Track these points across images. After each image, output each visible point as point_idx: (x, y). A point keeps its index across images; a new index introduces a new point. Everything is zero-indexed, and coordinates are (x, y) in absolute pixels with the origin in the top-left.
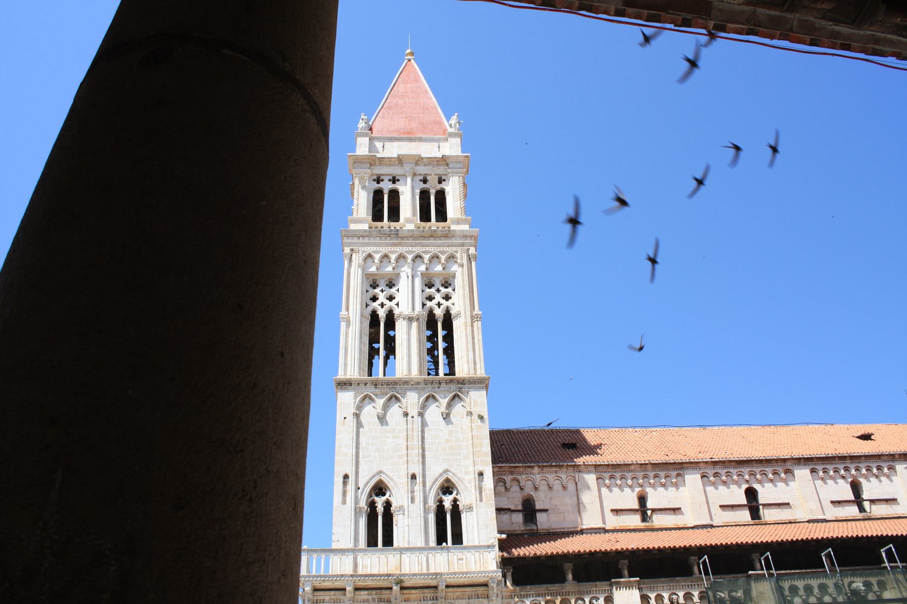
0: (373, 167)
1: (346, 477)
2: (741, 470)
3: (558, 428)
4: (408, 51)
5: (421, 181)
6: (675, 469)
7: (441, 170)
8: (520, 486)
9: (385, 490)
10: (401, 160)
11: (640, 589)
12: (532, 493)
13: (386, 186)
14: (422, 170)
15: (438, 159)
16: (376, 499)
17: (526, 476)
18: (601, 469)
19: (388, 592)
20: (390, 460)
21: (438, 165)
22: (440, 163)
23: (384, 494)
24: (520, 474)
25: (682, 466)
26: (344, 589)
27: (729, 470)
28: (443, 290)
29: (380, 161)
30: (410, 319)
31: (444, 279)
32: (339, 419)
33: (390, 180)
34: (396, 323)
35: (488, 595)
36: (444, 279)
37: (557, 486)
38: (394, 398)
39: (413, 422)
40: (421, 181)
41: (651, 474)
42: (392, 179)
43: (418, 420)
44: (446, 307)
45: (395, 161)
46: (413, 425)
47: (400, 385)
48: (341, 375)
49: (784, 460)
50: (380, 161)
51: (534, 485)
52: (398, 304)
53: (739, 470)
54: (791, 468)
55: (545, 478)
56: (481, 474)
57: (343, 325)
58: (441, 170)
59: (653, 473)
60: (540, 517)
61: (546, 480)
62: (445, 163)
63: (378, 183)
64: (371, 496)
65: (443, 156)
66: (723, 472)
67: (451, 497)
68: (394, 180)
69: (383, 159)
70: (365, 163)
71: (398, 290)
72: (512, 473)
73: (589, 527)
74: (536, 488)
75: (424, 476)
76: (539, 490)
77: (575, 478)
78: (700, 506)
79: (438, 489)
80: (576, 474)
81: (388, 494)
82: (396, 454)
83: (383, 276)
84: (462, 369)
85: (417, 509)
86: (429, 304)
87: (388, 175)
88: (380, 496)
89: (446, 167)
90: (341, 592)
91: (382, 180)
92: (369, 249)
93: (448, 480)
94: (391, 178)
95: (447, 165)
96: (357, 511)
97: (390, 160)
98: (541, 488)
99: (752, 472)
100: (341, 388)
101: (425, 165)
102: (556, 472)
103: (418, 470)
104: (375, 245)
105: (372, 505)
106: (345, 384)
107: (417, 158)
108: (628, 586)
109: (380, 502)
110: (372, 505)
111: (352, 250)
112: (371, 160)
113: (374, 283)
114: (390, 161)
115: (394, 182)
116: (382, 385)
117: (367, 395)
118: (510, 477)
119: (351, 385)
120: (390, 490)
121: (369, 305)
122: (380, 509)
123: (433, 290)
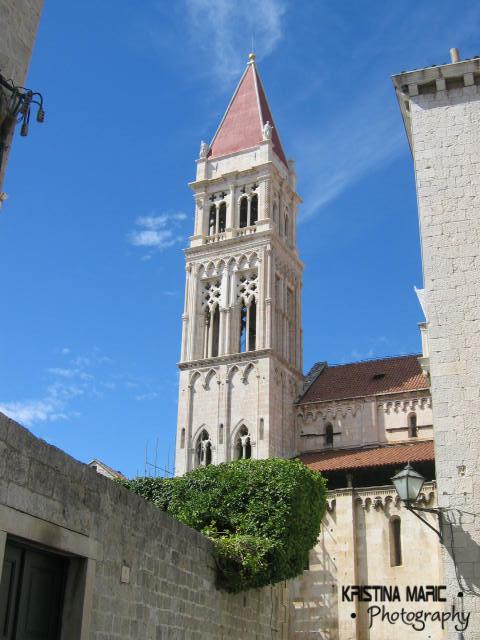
1: (184, 430)
4: (250, 55)
11: (354, 494)
12: (332, 422)
14: (241, 182)
24: (322, 408)
30: (225, 311)
32: (181, 392)
43: (226, 386)
48: (182, 362)
56: (262, 420)
57: (184, 323)
60: (336, 439)
67: (246, 437)
68: (223, 195)
72: (317, 408)
75: (228, 425)
84: (259, 346)
85: (223, 447)
92: (201, 261)
93: (244, 426)
96: (190, 452)
103: (224, 421)
104: (205, 256)
105: (199, 446)
108: (345, 493)
109: (204, 443)
110: (199, 446)
118: (316, 411)
122: (204, 448)
123: (244, 284)
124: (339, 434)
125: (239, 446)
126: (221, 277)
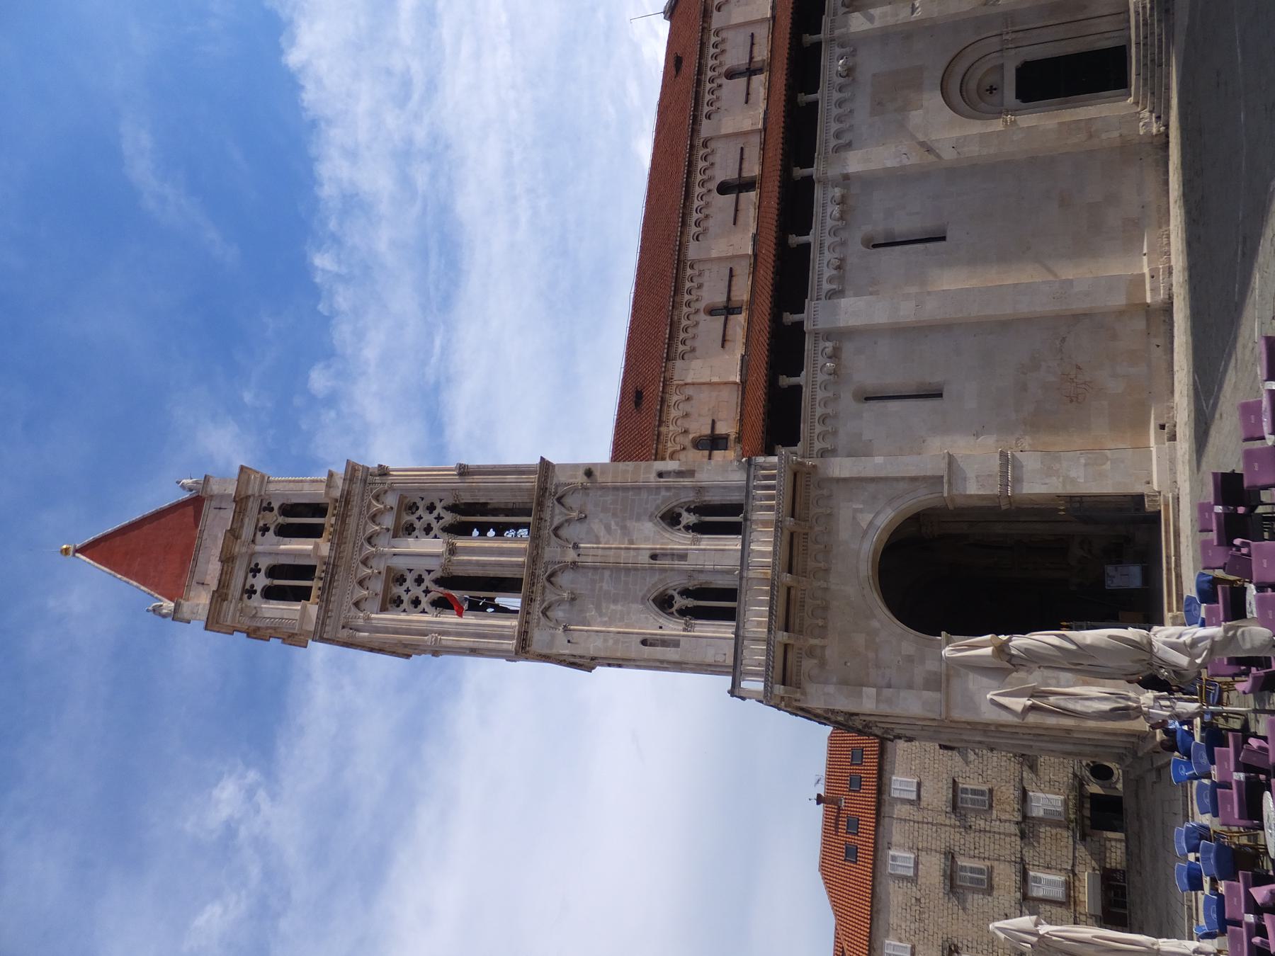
0: (230, 597)
1: (644, 642)
2: (696, 196)
3: (616, 417)
5: (263, 535)
6: (684, 269)
7: (253, 506)
8: (681, 450)
9: (666, 595)
10: (229, 558)
12: (691, 436)
13: (261, 581)
15: (238, 510)
16: (676, 606)
17: (669, 442)
18: (672, 355)
19: (793, 592)
20: (630, 586)
21: (245, 510)
22: (243, 507)
23: (672, 597)
24: (665, 449)
25: (681, 261)
26: (786, 646)
27: (695, 209)
28: (420, 512)
29: (224, 586)
31: (405, 510)
33: (254, 576)
34: (455, 574)
35: (807, 474)
36: (405, 510)
37: (684, 407)
38: (552, 579)
39: (585, 555)
40: (263, 535)
41: (687, 297)
42: (252, 574)
44: (444, 510)
45: (228, 566)
46: (589, 555)
47: (535, 569)
49: (692, 146)
50: (224, 586)
51: (682, 433)
52: (429, 572)
53: (696, 198)
54: (702, 140)
55: (674, 421)
58: (253, 506)
59: (686, 295)
60: (722, 429)
61: (677, 420)
62: (245, 500)
63: (255, 592)
64: (672, 613)
65: (234, 501)
66: (695, 216)
67: (685, 514)
69: (222, 583)
70: (221, 606)
71: (410, 570)
73: (738, 373)
74: (685, 431)
76: (688, 429)
77: (678, 385)
78: (731, 245)
79: (672, 529)
80: (675, 382)
81: (671, 592)
82: (623, 579)
83: (387, 589)
86: (436, 530)
87: (246, 578)
88: (674, 602)
89: (252, 499)
90: (789, 649)
91: (252, 586)
92: (348, 602)
94: (250, 575)
95: (248, 497)
97: (224, 573)
98: (687, 426)
99: (701, 183)
100: (529, 646)
101: (242, 526)
102: (669, 406)
105: (683, 612)
106: (524, 639)
107: (228, 534)
109: (680, 602)
111: (343, 627)
112: (219, 599)
113: (395, 602)
114: (226, 574)
115: (259, 571)
116: (532, 592)
117: (542, 612)
119: (527, 632)
120: (666, 589)
121: (424, 609)
122: (690, 603)
123: (418, 524)
124: (714, 422)
125: (701, 528)
126: (389, 569)
